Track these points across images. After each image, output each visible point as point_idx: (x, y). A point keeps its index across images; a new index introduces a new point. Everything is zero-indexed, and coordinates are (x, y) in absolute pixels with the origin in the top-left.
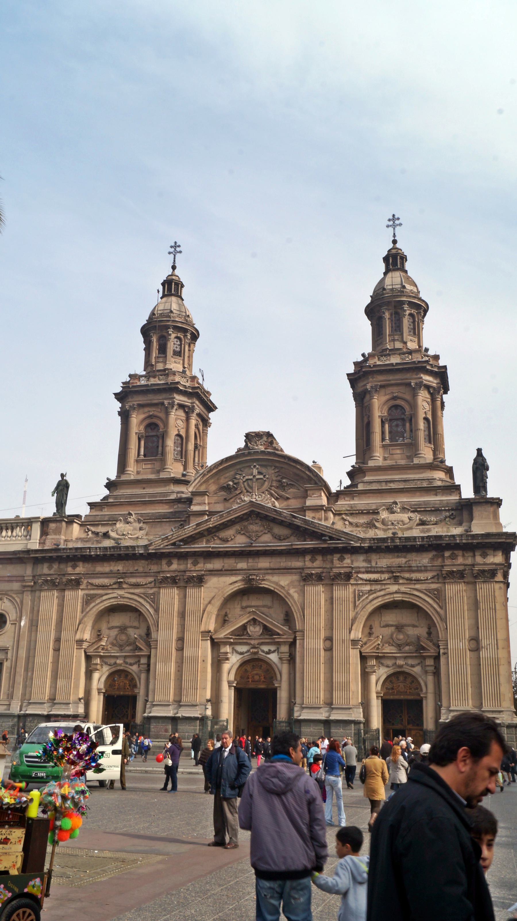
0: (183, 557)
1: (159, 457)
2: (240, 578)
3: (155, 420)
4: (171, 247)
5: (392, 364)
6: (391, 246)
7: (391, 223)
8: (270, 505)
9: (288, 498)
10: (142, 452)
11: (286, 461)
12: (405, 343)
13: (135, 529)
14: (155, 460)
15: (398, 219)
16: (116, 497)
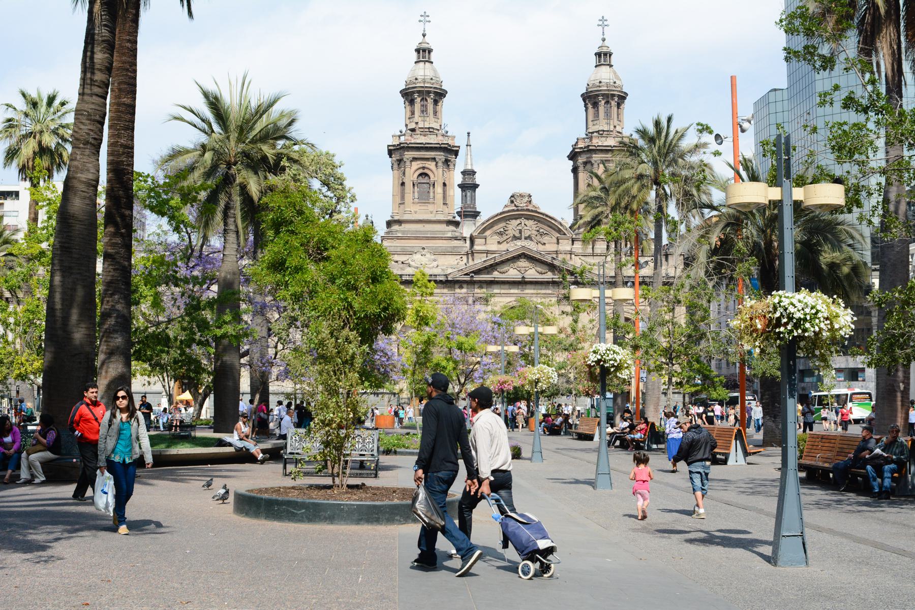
0: (471, 283)
1: (431, 200)
2: (513, 299)
3: (426, 171)
4: (421, 16)
5: (610, 146)
6: (600, 43)
7: (601, 23)
8: (535, 249)
9: (545, 244)
10: (416, 197)
11: (544, 217)
12: (615, 127)
13: (430, 260)
14: (429, 203)
15: (606, 20)
16: (403, 232)
